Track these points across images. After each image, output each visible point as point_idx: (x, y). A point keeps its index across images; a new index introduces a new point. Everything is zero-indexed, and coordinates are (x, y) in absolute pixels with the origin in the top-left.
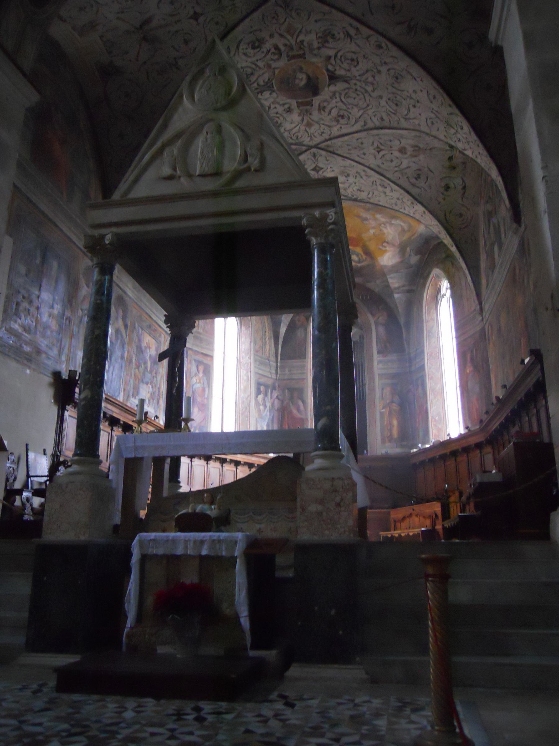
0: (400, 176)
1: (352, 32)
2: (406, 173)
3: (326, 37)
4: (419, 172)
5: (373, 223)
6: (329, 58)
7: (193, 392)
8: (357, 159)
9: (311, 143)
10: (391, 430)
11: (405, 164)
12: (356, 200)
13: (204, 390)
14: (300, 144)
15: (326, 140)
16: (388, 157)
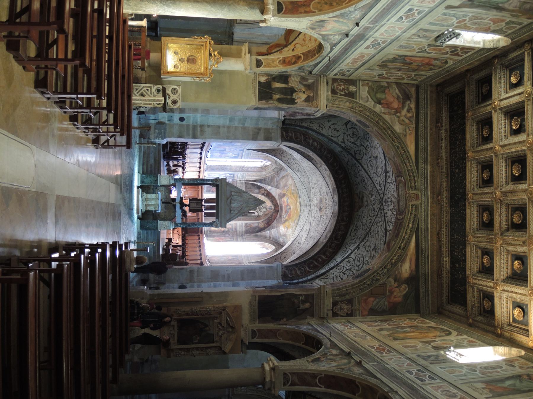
5: (293, 224)
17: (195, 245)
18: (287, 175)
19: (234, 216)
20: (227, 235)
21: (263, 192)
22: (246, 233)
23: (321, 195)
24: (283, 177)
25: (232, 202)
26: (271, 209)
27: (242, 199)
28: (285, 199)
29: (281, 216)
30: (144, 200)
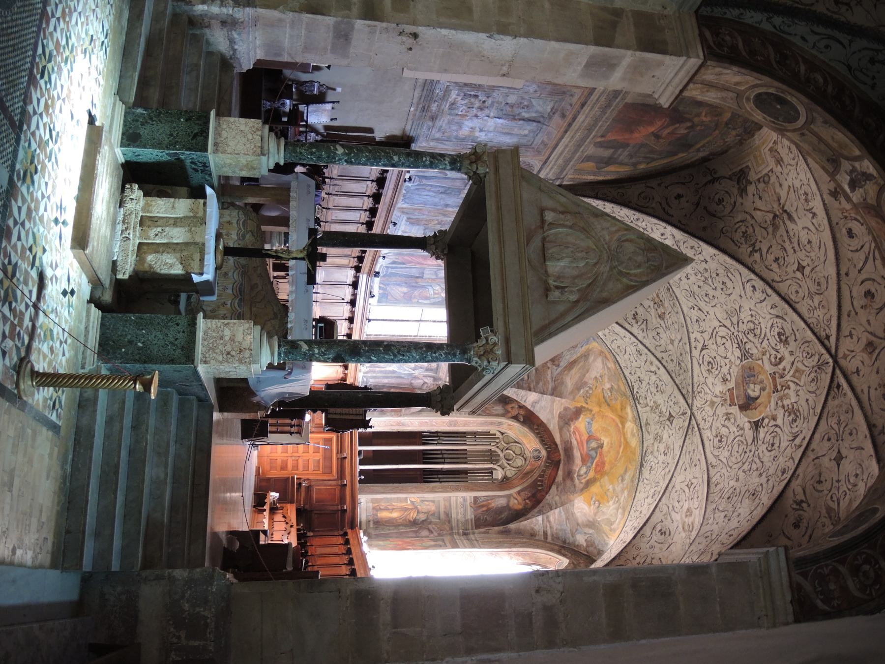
0: (664, 512)
1: (798, 441)
2: (666, 519)
3: (793, 412)
4: (667, 533)
5: (618, 488)
6: (775, 419)
7: (423, 287)
8: (681, 462)
9: (695, 408)
10: (386, 509)
11: (676, 517)
12: (642, 465)
13: (427, 298)
14: (693, 397)
15: (698, 425)
16: (683, 497)
17: (336, 560)
18: (586, 356)
19: (562, 315)
20: (425, 533)
21: (515, 412)
22: (477, 526)
23: (746, 355)
24: (572, 364)
25: (552, 250)
26: (538, 458)
27: (590, 243)
28: (581, 423)
29: (569, 475)
30: (134, 220)
